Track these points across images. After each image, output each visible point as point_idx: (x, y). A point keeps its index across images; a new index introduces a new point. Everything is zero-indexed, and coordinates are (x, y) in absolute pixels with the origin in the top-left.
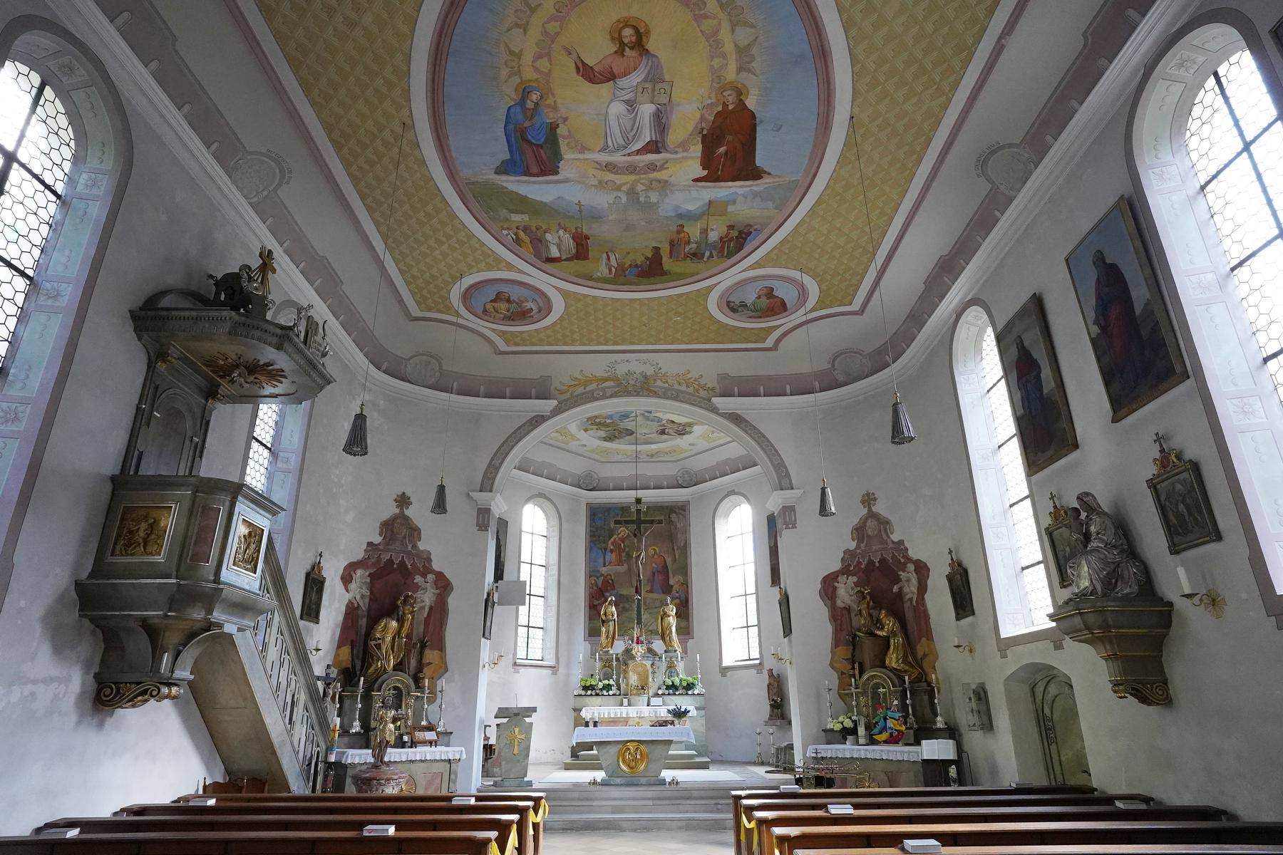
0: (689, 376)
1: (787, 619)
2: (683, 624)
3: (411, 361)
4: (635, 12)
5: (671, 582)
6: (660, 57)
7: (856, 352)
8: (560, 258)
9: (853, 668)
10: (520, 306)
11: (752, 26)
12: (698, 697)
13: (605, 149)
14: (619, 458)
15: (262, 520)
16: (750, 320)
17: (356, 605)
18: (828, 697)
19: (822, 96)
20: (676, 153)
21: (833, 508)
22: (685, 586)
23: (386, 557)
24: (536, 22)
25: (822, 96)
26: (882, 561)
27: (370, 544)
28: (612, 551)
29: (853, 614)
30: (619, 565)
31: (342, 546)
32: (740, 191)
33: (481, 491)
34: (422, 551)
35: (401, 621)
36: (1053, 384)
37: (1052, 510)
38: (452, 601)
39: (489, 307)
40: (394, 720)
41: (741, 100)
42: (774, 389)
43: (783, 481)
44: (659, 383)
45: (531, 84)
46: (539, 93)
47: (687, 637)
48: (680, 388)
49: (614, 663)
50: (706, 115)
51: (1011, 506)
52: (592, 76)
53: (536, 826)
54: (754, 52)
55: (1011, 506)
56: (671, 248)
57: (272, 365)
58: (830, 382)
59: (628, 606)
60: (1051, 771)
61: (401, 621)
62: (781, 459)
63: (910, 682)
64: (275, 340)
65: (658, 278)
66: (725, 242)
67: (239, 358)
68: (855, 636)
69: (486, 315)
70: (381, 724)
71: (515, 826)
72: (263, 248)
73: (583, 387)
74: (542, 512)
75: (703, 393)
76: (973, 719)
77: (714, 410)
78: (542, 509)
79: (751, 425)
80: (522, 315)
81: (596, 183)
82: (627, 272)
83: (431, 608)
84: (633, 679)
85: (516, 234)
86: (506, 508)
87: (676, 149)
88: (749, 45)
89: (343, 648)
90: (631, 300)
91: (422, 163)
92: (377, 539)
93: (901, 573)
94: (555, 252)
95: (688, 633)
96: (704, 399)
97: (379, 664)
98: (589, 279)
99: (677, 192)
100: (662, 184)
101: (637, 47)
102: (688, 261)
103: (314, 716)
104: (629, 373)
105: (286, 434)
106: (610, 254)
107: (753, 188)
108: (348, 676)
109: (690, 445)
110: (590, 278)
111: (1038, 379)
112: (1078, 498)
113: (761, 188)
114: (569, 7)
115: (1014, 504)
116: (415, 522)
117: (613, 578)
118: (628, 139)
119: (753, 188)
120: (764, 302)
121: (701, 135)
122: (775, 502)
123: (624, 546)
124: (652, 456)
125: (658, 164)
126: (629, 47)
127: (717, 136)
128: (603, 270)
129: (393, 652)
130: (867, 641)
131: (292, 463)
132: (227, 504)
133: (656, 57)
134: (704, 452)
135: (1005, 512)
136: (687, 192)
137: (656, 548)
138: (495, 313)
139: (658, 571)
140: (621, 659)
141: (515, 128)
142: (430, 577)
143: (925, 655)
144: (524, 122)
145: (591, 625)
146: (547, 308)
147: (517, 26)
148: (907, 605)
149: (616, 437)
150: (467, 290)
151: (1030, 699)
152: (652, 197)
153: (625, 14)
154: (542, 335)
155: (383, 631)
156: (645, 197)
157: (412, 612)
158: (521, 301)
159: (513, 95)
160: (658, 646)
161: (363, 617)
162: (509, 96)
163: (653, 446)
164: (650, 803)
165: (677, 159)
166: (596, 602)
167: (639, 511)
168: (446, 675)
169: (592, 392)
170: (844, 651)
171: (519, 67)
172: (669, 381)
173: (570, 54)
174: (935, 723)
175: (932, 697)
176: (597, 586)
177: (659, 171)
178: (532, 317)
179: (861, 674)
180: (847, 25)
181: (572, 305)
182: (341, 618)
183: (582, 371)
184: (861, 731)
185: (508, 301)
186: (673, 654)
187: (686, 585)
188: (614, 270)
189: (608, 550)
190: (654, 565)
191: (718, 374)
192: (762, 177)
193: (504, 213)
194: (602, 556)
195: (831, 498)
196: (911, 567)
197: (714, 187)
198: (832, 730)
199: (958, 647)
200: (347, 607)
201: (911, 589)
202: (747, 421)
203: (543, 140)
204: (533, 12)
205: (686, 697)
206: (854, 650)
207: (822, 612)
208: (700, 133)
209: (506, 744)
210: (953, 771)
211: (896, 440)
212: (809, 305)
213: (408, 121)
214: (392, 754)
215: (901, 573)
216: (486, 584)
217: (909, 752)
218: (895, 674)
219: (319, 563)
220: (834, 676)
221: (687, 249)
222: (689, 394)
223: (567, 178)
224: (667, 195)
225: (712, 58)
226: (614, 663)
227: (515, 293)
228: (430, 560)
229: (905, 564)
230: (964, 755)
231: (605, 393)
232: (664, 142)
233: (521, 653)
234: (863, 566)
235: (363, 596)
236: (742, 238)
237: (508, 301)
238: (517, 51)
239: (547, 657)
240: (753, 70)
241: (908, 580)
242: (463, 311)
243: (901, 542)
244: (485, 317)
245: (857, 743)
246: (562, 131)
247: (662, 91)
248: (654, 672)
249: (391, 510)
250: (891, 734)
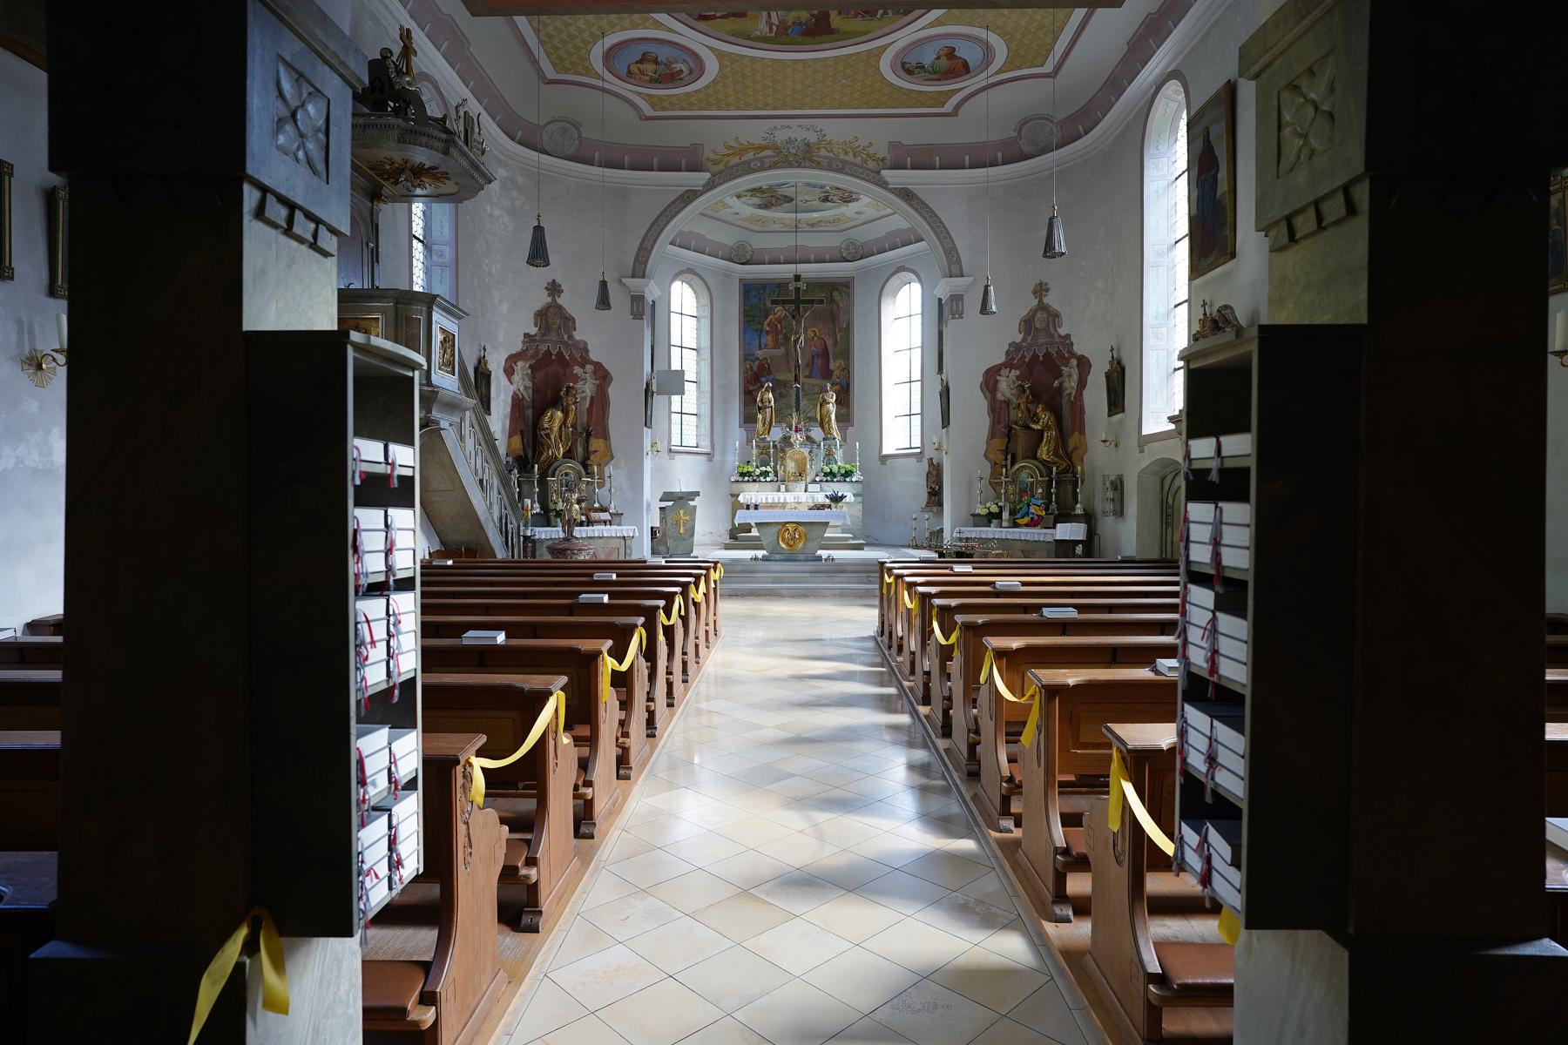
0: (857, 144)
1: (946, 410)
2: (843, 411)
3: (546, 129)
5: (832, 367)
7: (1046, 119)
9: (1006, 459)
10: (669, 68)
12: (856, 485)
14: (776, 227)
15: (452, 326)
16: (926, 83)
17: (521, 396)
18: (978, 485)
21: (994, 307)
22: (846, 371)
23: (543, 348)
26: (1047, 354)
27: (526, 335)
28: (767, 333)
29: (1011, 408)
31: (501, 338)
33: (633, 277)
34: (579, 342)
35: (566, 412)
36: (1226, 188)
37: (1202, 317)
38: (612, 391)
39: (634, 68)
40: (579, 502)
42: (952, 160)
43: (954, 267)
44: (823, 152)
47: (846, 424)
48: (846, 158)
49: (772, 451)
51: (1176, 306)
53: (715, 582)
55: (1176, 306)
57: (437, 168)
58: (1014, 154)
59: (786, 392)
60: (1164, 550)
61: (566, 412)
62: (953, 242)
63: (1057, 473)
64: (440, 145)
65: (824, 38)
67: (406, 163)
68: (1011, 428)
69: (630, 77)
70: (567, 505)
71: (703, 577)
72: (401, 28)
73: (738, 157)
74: (690, 289)
75: (871, 165)
76: (1109, 507)
77: (883, 184)
78: (691, 286)
79: (923, 203)
80: (670, 77)
82: (790, 31)
83: (592, 398)
84: (791, 466)
86: (660, 294)
89: (514, 437)
90: (796, 61)
92: (533, 330)
93: (1063, 368)
95: (849, 421)
96: (872, 172)
97: (550, 452)
98: (746, 37)
102: (859, 18)
103: (505, 498)
104: (790, 141)
105: (435, 225)
108: (523, 463)
109: (857, 213)
110: (748, 38)
111: (1215, 177)
112: (1218, 311)
115: (1179, 304)
116: (568, 311)
120: (944, 63)
122: (944, 289)
124: (813, 225)
128: (762, 28)
129: (561, 440)
130: (1021, 434)
131: (447, 257)
132: (424, 314)
134: (872, 221)
135: (1169, 313)
137: (816, 330)
142: (589, 368)
143: (1075, 448)
146: (699, 68)
148: (1065, 400)
149: (772, 204)
150: (610, 50)
151: (1158, 489)
154: (693, 99)
155: (550, 421)
157: (575, 403)
158: (669, 62)
160: (817, 433)
161: (528, 407)
163: (815, 215)
164: (808, 575)
166: (751, 388)
167: (797, 289)
168: (612, 462)
169: (749, 162)
170: (999, 443)
174: (1074, 509)
175: (1075, 486)
178: (681, 79)
179: (1013, 464)
181: (727, 67)
182: (508, 409)
183: (737, 138)
184: (1005, 515)
185: (656, 62)
186: (833, 441)
187: (847, 370)
188: (774, 28)
190: (813, 348)
191: (890, 142)
195: (993, 298)
196: (1074, 362)
198: (979, 515)
199: (1104, 441)
200: (513, 398)
201: (1071, 384)
202: (918, 198)
205: (843, 484)
206: (1009, 442)
207: (981, 403)
209: (672, 524)
210: (1079, 549)
211: (1048, 254)
212: (993, 68)
214: (579, 532)
215: (1063, 368)
216: (645, 376)
217: (1045, 534)
218: (1043, 465)
219: (484, 356)
220: (987, 466)
222: (855, 165)
226: (772, 451)
227: (663, 53)
228: (587, 351)
229: (1068, 359)
230: (1096, 538)
231: (763, 164)
233: (675, 440)
234: (1027, 360)
235: (526, 388)
237: (656, 62)
239: (702, 444)
241: (1070, 376)
242: (607, 76)
243: (1068, 336)
245: (1001, 527)
248: (812, 460)
249: (544, 299)
250: (1032, 519)
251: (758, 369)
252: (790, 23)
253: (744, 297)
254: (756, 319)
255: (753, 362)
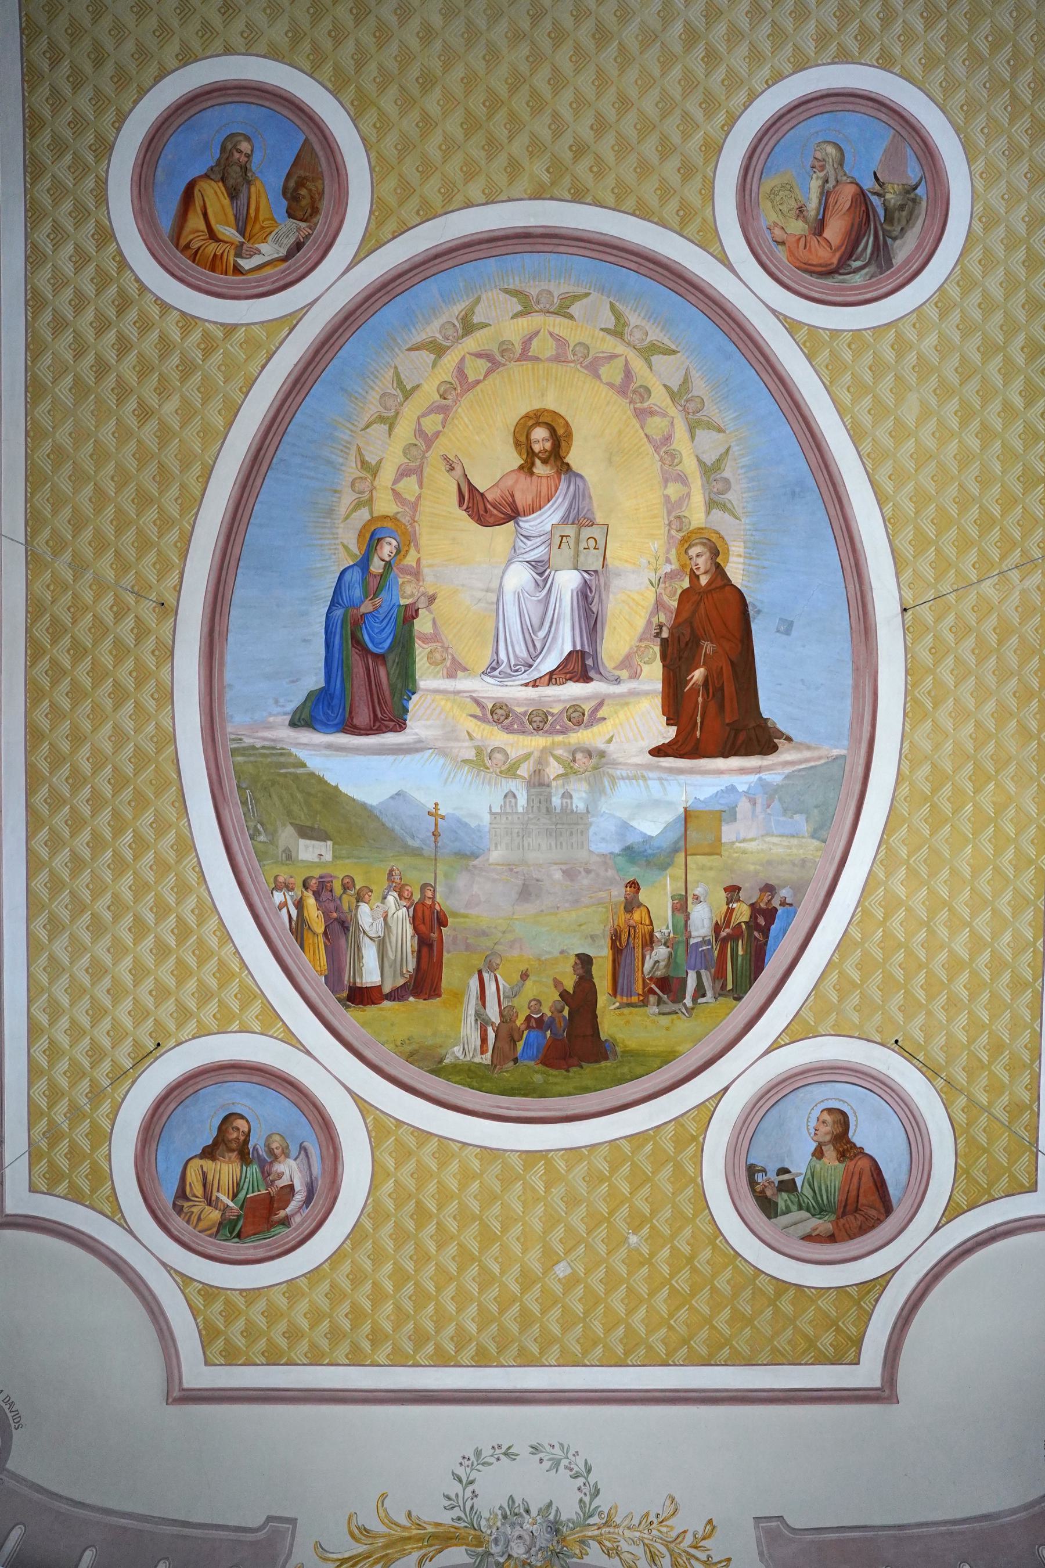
0: (678, 1524)
4: (550, 402)
6: (586, 477)
8: (379, 988)
11: (720, 430)
13: (492, 669)
19: (846, 564)
20: (618, 681)
24: (410, 412)
25: (846, 564)
32: (743, 783)
41: (718, 566)
45: (385, 525)
46: (394, 543)
50: (665, 598)
52: (482, 512)
54: (727, 474)
56: (614, 955)
65: (588, 1072)
66: (725, 941)
81: (471, 755)
82: (520, 1045)
85: (300, 905)
87: (617, 673)
88: (718, 460)
91: (167, 696)
94: (371, 975)
99: (622, 782)
100: (594, 760)
101: (552, 459)
106: (485, 975)
107: (766, 776)
113: (774, 778)
114: (459, 389)
118: (534, 646)
119: (763, 775)
121: (659, 640)
125: (587, 707)
126: (540, 458)
127: (687, 644)
133: (581, 477)
136: (641, 782)
138: (203, 1205)
141: (345, 615)
144: (362, 602)
147: (381, 419)
152: (575, 796)
153: (537, 405)
156: (563, 796)
158: (271, 1152)
159: (356, 551)
162: (346, 547)
165: (621, 696)
171: (371, 491)
172: (624, 1546)
173: (453, 469)
177: (590, 725)
178: (286, 1222)
180: (856, 435)
185: (244, 1155)
191: (757, 1519)
192: (774, 749)
193: (287, 835)
197: (691, 771)
203: (386, 645)
204: (406, 398)
208: (658, 635)
213: (171, 600)
221: (648, 964)
223: (420, 741)
224: (603, 792)
225: (666, 481)
232: (595, 657)
236: (758, 927)
238: (374, 463)
240: (729, 506)
244: (178, 1223)
246: (422, 625)
247: (592, 542)
252: (520, 1022)
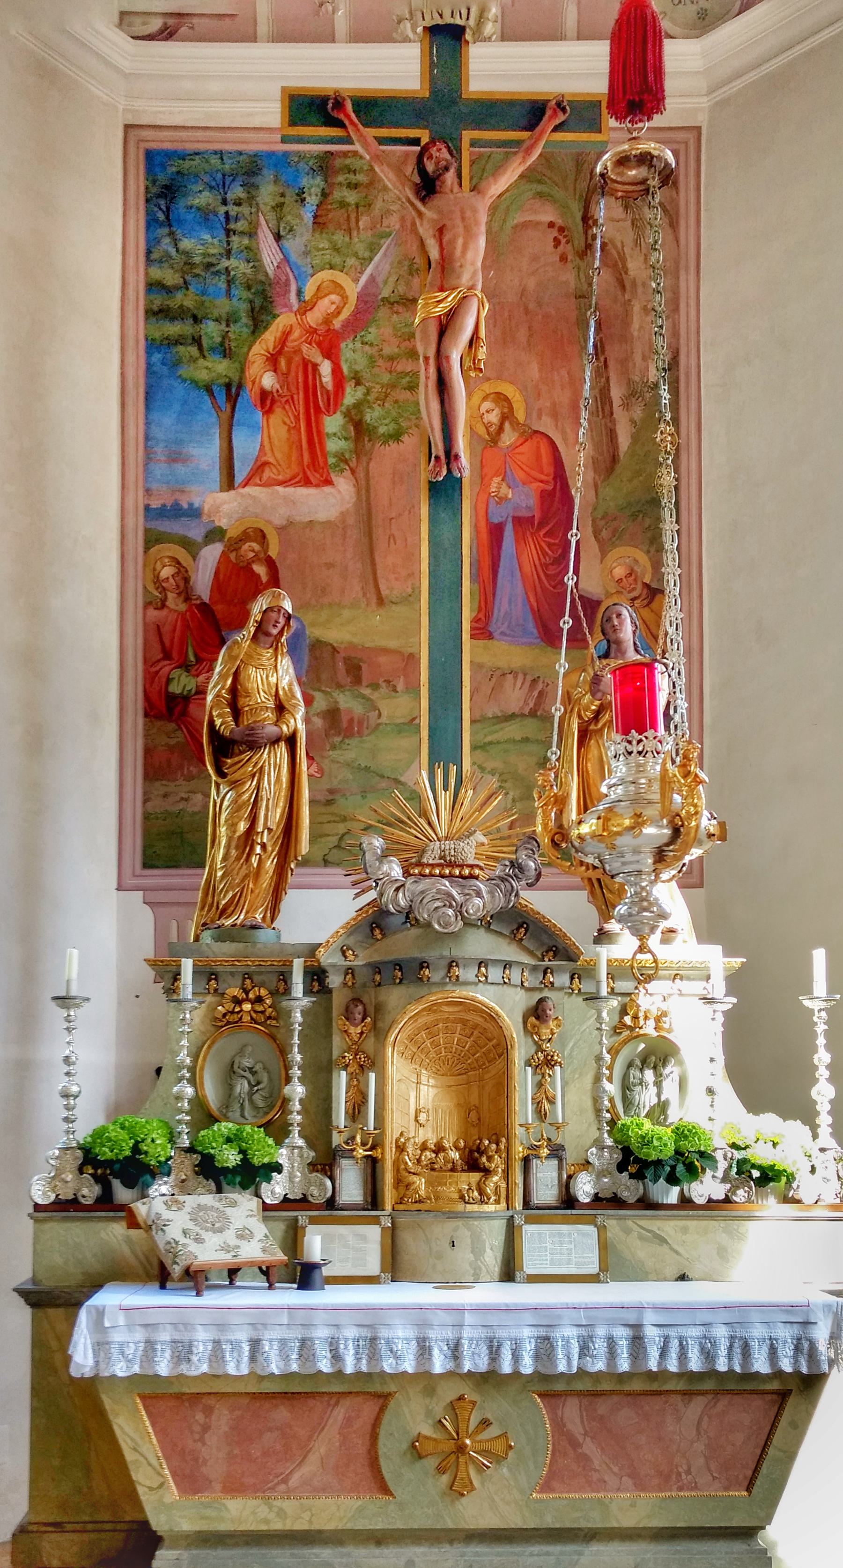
30: (307, 482)
117: (273, 553)
123: (337, 371)
137: (509, 390)
139: (518, 521)
140: (334, 980)
145: (157, 805)
176: (185, 589)
189: (248, 396)
194: (216, 433)
251: (218, 584)
253: (151, 223)
254: (211, 330)
255: (191, 547)
